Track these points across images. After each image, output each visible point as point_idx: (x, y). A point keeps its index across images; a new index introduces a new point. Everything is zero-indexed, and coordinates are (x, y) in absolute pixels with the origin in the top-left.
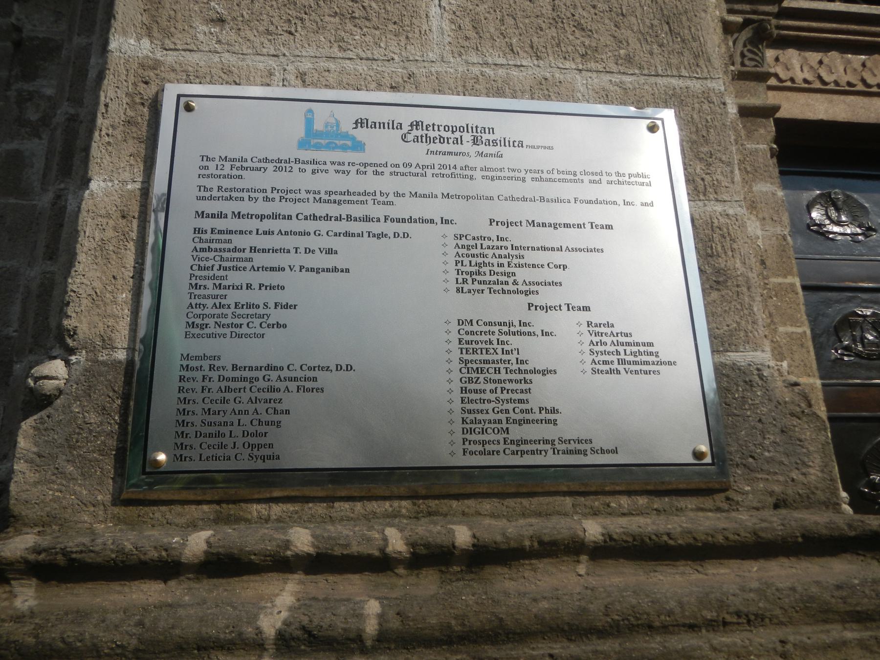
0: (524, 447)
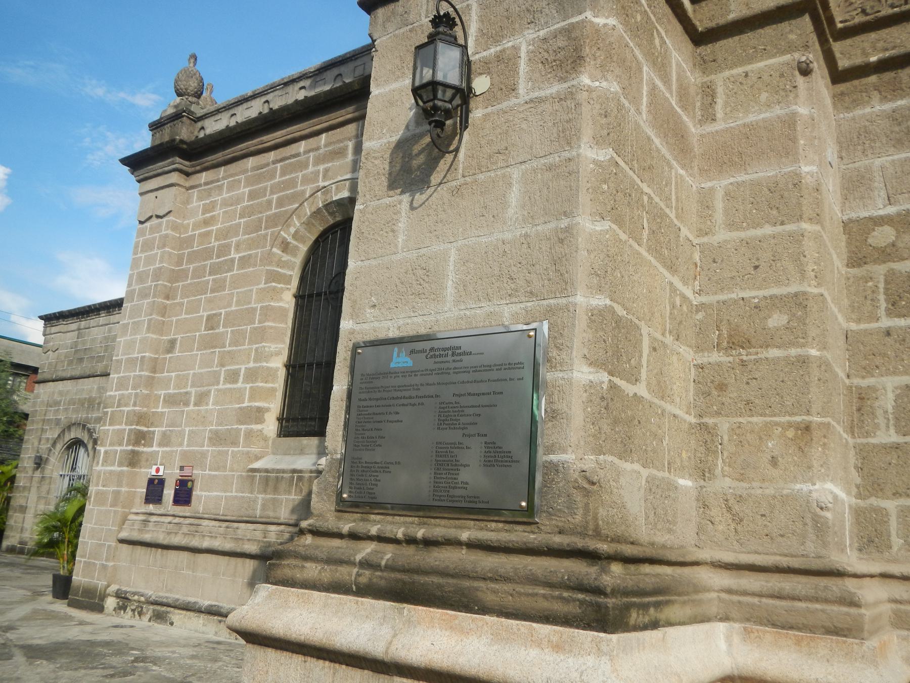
0: (454, 499)
